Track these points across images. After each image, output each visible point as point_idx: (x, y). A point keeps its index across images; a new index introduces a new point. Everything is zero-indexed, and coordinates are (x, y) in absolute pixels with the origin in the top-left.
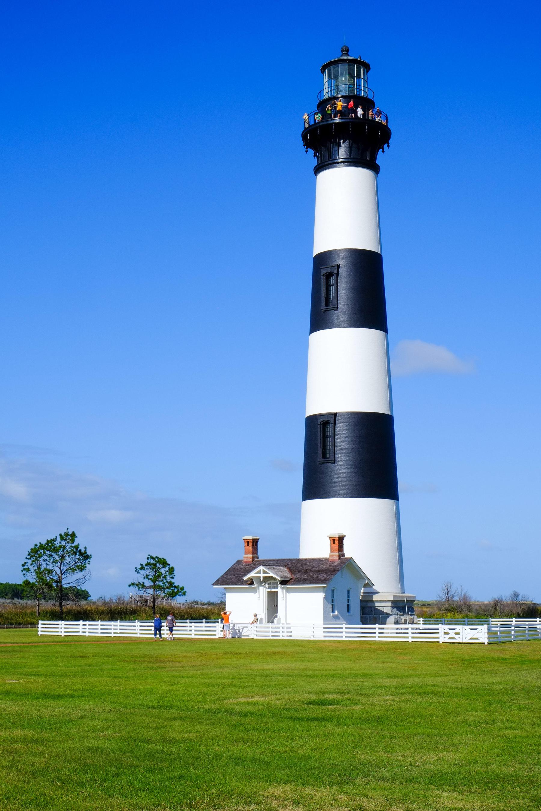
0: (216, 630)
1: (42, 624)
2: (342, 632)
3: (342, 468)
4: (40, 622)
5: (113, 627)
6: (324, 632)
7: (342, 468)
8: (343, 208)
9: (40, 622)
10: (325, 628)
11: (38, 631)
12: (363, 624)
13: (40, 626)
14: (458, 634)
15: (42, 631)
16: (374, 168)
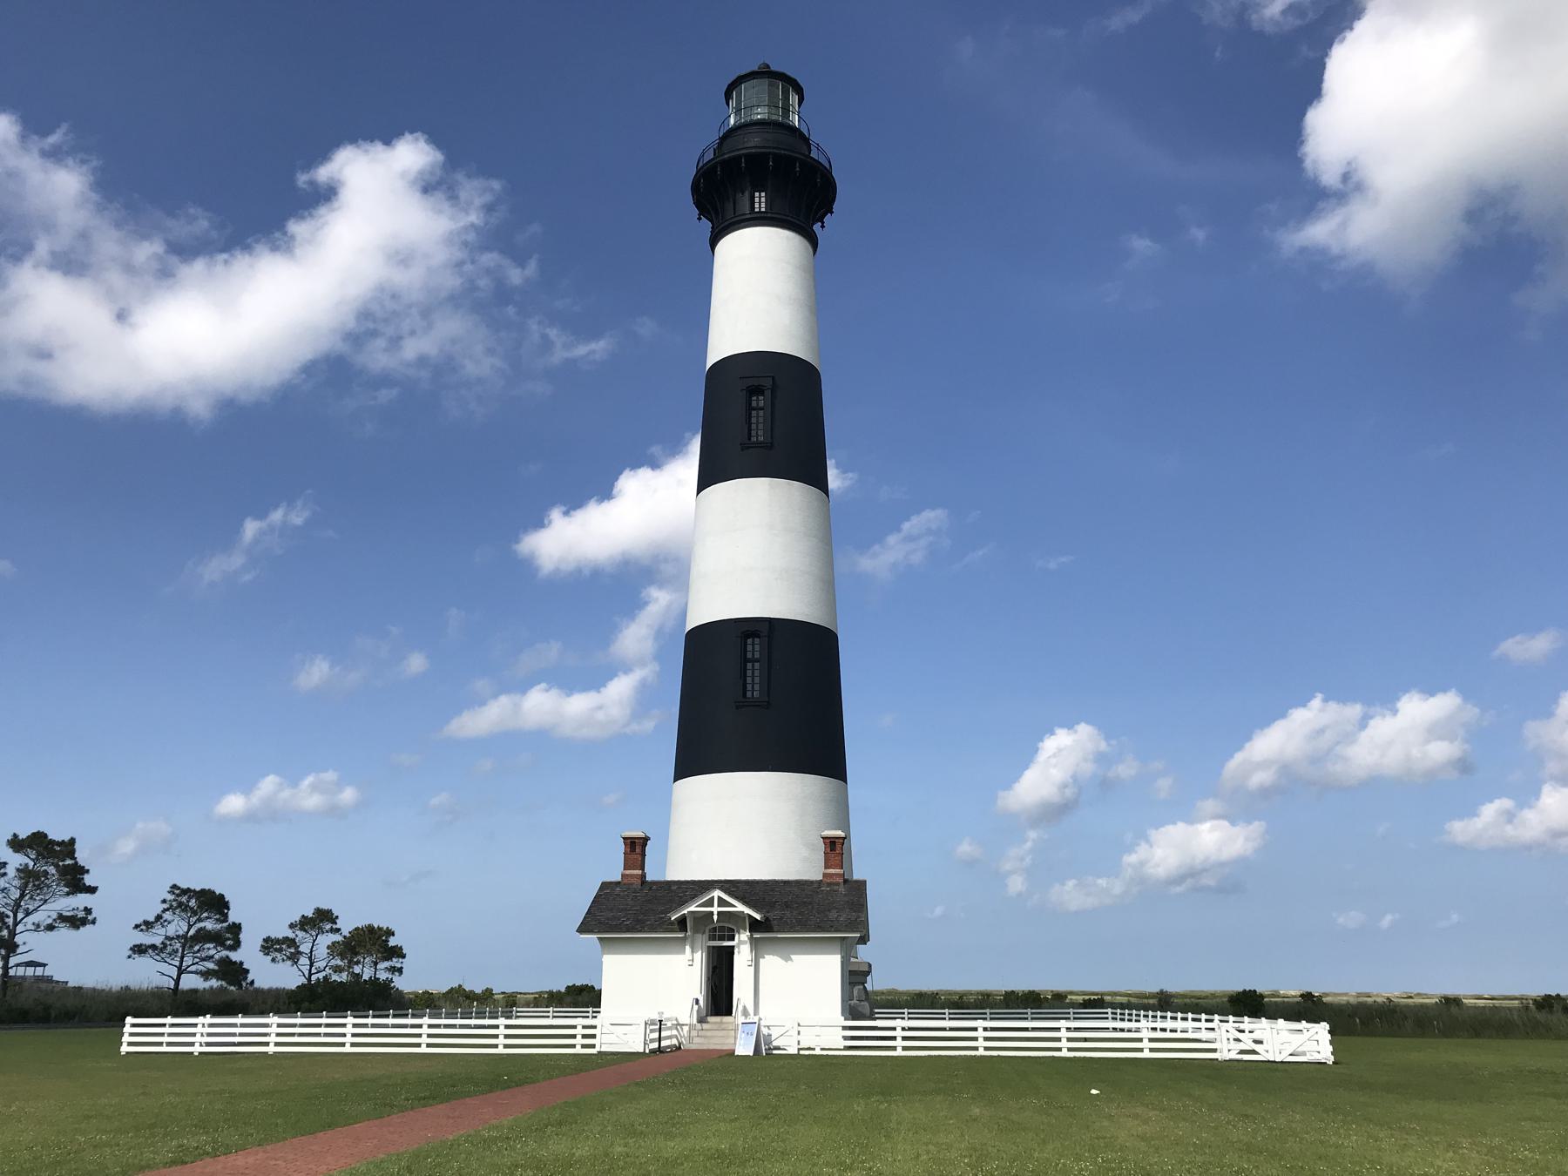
1: (134, 1025)
2: (1059, 1039)
4: (129, 1020)
6: (845, 1038)
9: (129, 1020)
10: (845, 1028)
12: (854, 1019)
13: (127, 1029)
14: (1261, 1042)
15: (130, 1044)
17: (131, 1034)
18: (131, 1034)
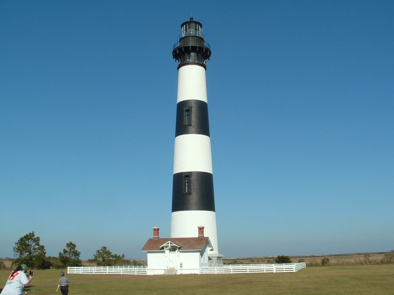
0: (135, 271)
1: (69, 268)
3: (194, 197)
4: (68, 267)
5: (93, 270)
7: (194, 197)
8: (192, 82)
9: (68, 267)
11: (67, 272)
13: (68, 269)
16: (204, 67)
17: (69, 270)
18: (69, 270)
